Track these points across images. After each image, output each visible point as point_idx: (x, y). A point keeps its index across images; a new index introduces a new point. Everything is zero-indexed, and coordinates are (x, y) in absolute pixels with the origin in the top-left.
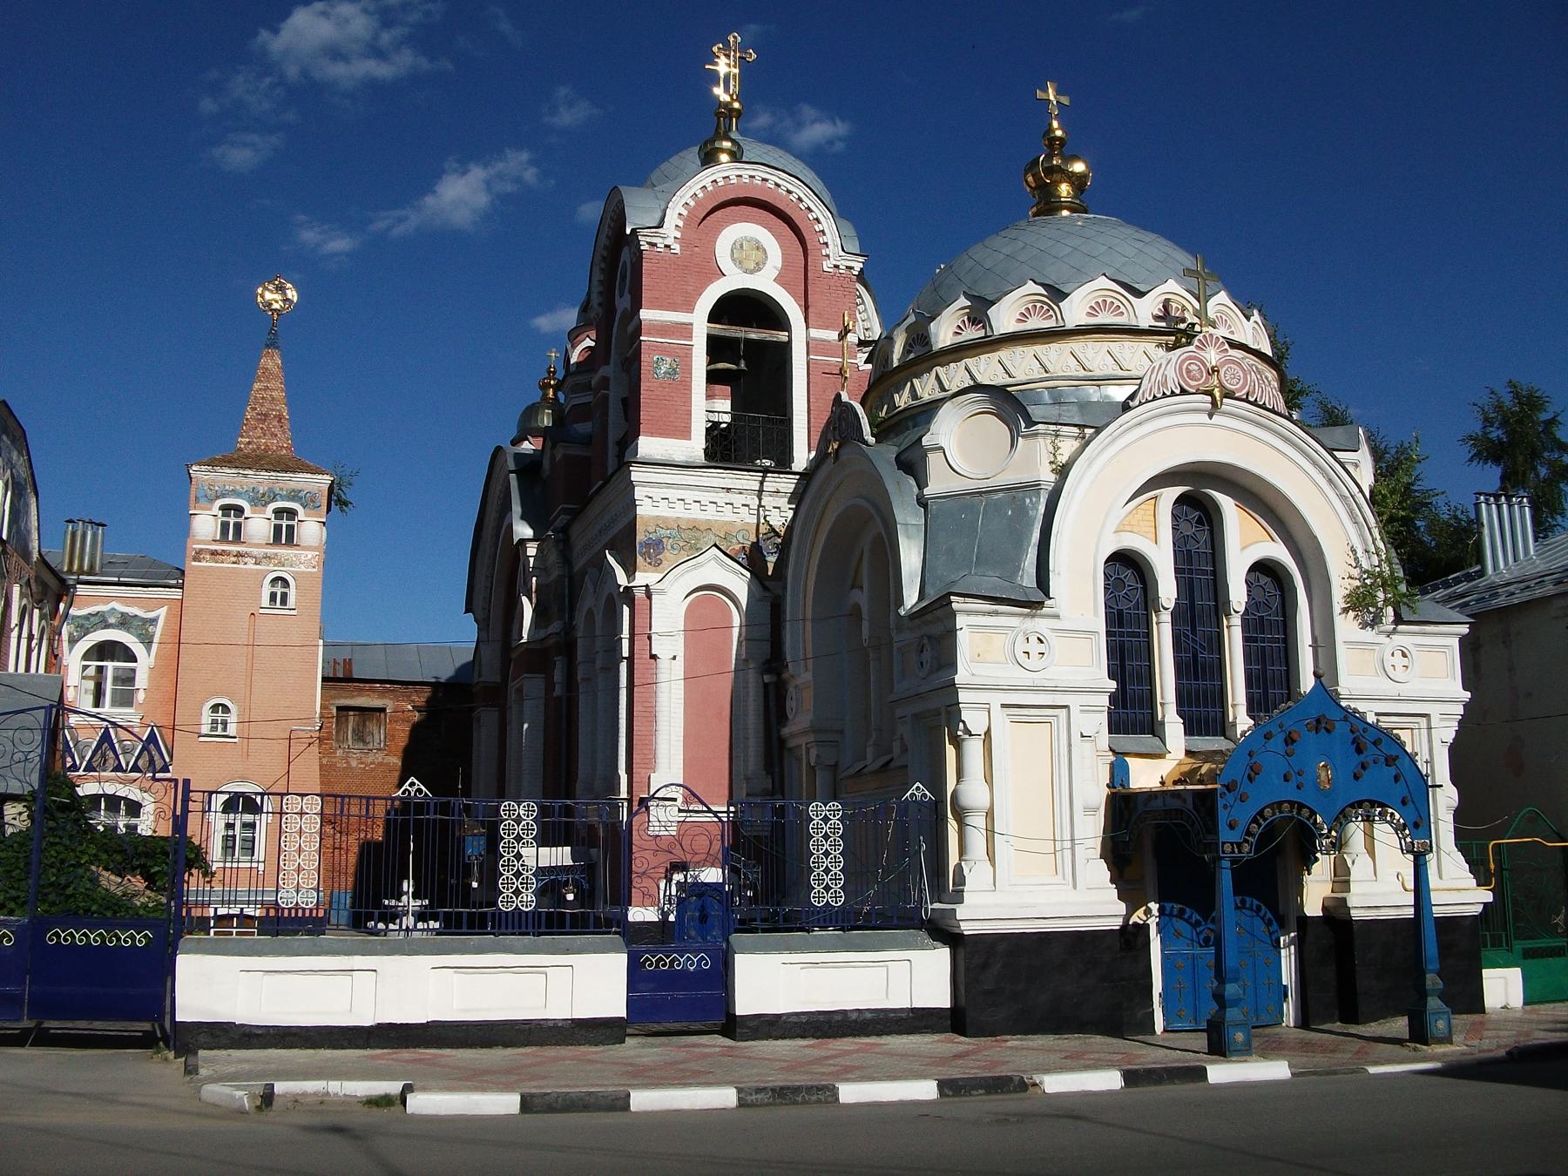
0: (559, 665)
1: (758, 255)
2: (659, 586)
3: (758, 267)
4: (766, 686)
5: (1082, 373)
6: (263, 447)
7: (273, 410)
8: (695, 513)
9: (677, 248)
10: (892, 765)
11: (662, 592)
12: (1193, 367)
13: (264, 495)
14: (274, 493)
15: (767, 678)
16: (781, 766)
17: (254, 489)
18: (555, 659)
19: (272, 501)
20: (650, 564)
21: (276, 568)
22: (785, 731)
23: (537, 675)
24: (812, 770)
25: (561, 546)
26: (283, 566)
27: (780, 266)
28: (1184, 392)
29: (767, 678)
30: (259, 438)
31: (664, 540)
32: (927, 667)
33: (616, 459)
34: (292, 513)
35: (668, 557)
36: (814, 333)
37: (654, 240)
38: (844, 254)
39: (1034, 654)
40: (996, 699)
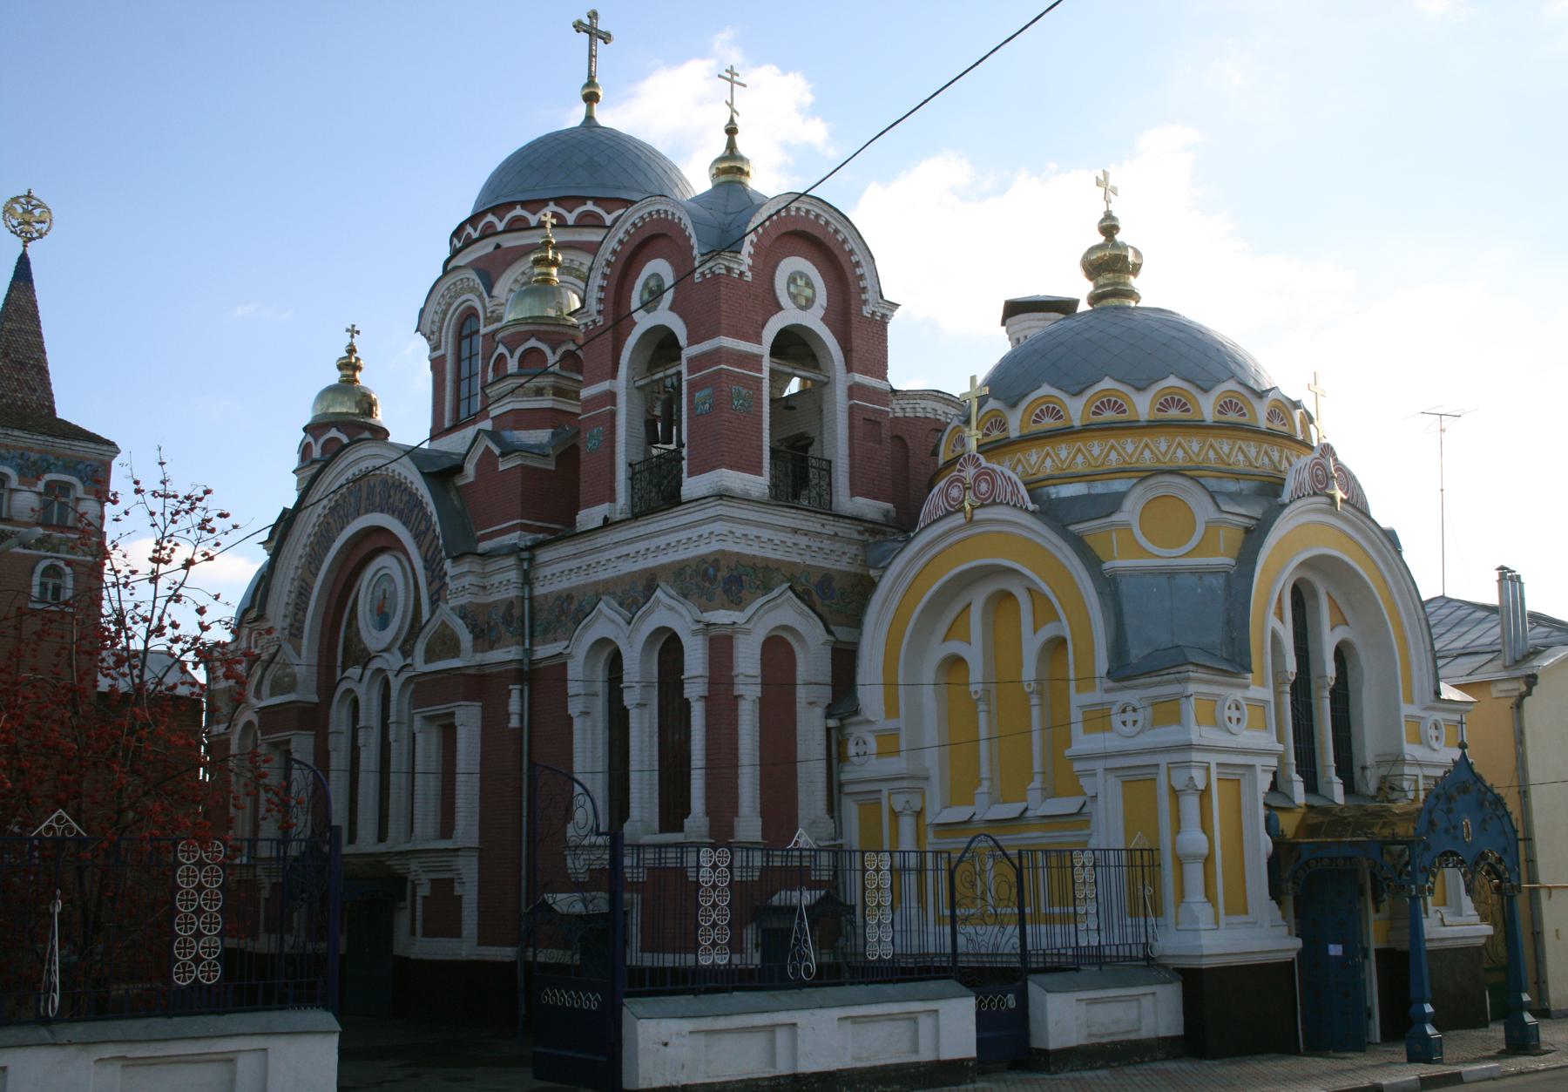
0: (515, 695)
1: (808, 292)
2: (747, 626)
3: (810, 302)
4: (828, 730)
5: (1222, 467)
6: (19, 403)
7: (29, 358)
8: (769, 553)
9: (749, 276)
10: (1029, 813)
11: (748, 632)
12: (1319, 472)
13: (34, 463)
14: (47, 461)
15: (832, 723)
16: (840, 811)
17: (22, 454)
18: (511, 687)
19: (45, 472)
20: (732, 601)
21: (49, 554)
22: (844, 777)
23: (475, 703)
24: (895, 815)
25: (525, 566)
26: (57, 552)
27: (825, 305)
28: (1315, 494)
29: (832, 723)
30: (15, 391)
31: (744, 578)
32: (1139, 724)
33: (629, 482)
34: (66, 488)
35: (744, 594)
36: (859, 378)
37: (732, 265)
38: (880, 301)
39: (1234, 720)
40: (1214, 759)
